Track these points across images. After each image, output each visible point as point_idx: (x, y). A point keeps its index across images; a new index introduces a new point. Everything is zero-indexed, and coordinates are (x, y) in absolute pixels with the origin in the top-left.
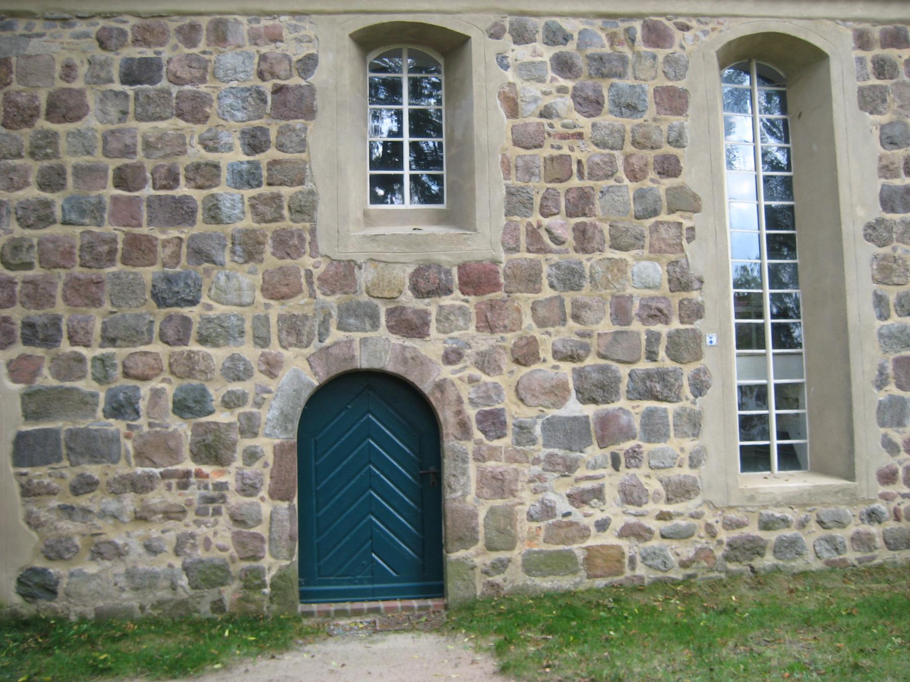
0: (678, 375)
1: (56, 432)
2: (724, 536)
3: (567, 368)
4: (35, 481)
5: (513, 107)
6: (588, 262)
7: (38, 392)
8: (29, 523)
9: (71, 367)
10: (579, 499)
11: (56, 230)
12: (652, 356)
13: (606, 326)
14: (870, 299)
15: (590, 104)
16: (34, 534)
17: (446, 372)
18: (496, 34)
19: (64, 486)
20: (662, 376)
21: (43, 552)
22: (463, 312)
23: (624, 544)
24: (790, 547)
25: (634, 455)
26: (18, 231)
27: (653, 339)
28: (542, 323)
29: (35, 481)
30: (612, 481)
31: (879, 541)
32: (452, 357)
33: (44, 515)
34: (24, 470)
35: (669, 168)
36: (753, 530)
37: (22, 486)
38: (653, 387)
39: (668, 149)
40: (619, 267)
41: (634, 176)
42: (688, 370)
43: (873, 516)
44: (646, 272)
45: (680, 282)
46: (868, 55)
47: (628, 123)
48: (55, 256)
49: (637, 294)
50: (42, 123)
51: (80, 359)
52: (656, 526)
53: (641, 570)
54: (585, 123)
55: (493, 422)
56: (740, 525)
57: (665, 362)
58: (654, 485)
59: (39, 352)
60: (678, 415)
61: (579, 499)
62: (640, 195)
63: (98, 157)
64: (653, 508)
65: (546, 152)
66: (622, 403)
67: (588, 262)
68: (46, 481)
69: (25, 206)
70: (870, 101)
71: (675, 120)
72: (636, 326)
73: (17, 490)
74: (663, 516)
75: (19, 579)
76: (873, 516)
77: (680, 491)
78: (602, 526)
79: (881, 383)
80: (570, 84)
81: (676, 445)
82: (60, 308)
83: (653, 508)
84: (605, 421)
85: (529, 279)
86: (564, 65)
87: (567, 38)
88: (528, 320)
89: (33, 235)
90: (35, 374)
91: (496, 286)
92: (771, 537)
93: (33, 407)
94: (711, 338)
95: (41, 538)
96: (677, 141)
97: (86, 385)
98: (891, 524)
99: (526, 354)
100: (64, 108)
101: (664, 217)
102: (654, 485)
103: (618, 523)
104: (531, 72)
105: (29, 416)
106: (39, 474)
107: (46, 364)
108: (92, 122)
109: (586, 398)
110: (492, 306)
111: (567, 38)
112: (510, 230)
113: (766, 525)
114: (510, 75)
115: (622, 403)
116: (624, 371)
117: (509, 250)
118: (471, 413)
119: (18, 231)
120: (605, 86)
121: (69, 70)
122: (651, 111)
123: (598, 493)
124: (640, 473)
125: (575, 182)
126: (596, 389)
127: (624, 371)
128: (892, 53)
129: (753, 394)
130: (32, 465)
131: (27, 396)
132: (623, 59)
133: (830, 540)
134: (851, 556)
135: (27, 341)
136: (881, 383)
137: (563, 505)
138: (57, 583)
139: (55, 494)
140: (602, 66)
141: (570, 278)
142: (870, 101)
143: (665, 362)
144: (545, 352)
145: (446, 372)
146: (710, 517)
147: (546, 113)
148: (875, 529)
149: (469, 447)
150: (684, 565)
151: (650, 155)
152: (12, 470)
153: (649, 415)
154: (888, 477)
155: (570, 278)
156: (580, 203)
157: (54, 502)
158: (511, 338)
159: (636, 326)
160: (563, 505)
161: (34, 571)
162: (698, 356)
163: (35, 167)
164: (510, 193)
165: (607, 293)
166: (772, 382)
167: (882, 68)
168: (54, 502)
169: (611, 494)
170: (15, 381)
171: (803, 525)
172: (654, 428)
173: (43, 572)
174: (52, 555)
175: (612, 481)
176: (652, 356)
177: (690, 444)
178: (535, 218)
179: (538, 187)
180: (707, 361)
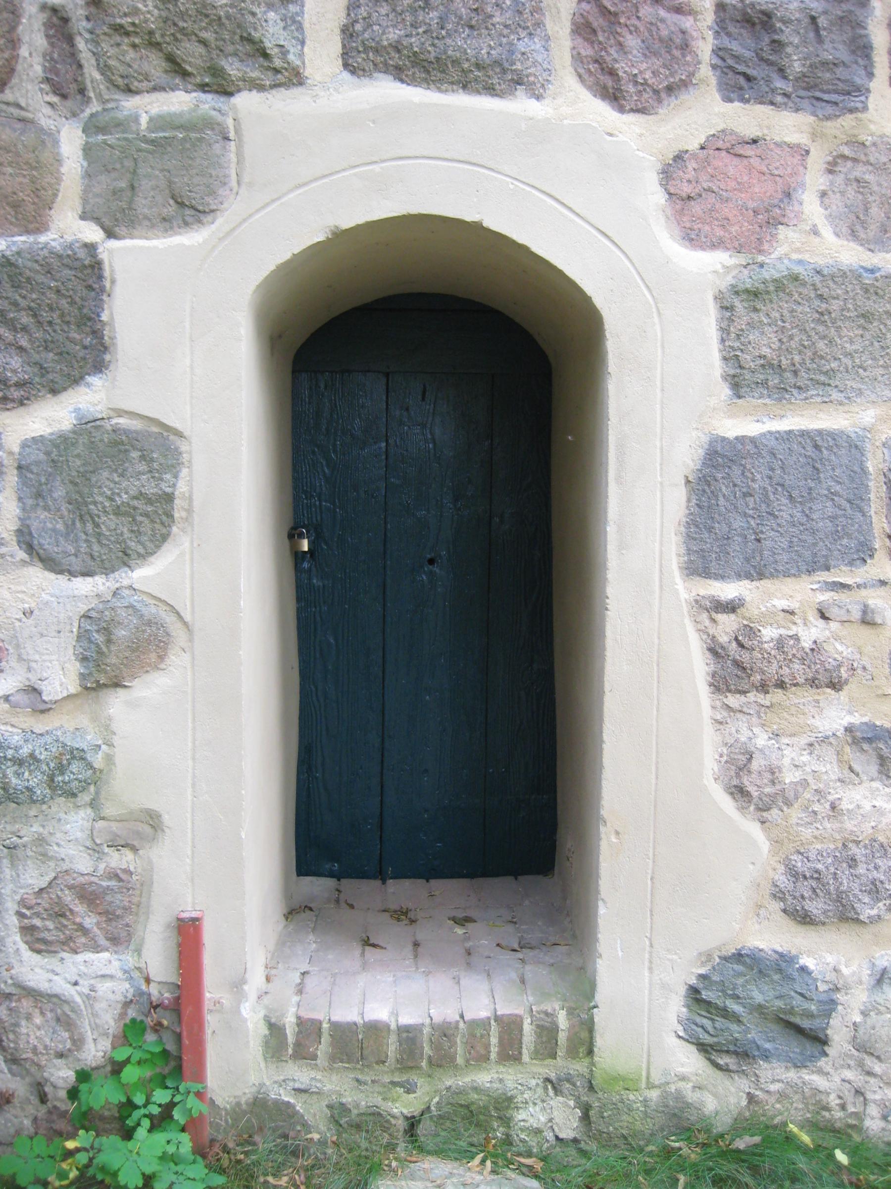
1: (854, 445)
4: (769, 633)
7: (786, 285)
8: (739, 792)
16: (754, 829)
21: (778, 895)
29: (769, 633)
33: (793, 761)
34: (728, 590)
37: (715, 651)
59: (788, 126)
68: (811, 632)
73: (700, 666)
75: (694, 994)
90: (772, 217)
93: (764, 343)
95: (777, 842)
105: (744, 379)
106: (784, 605)
107: (814, 178)
130: (757, 572)
131: (745, 301)
135: (739, 82)
138: (830, 1006)
139: (836, 685)
152: (686, 590)
157: (835, 715)
161: (745, 960)
168: (835, 715)
170: (692, 238)
173: (782, 967)
174: (815, 907)
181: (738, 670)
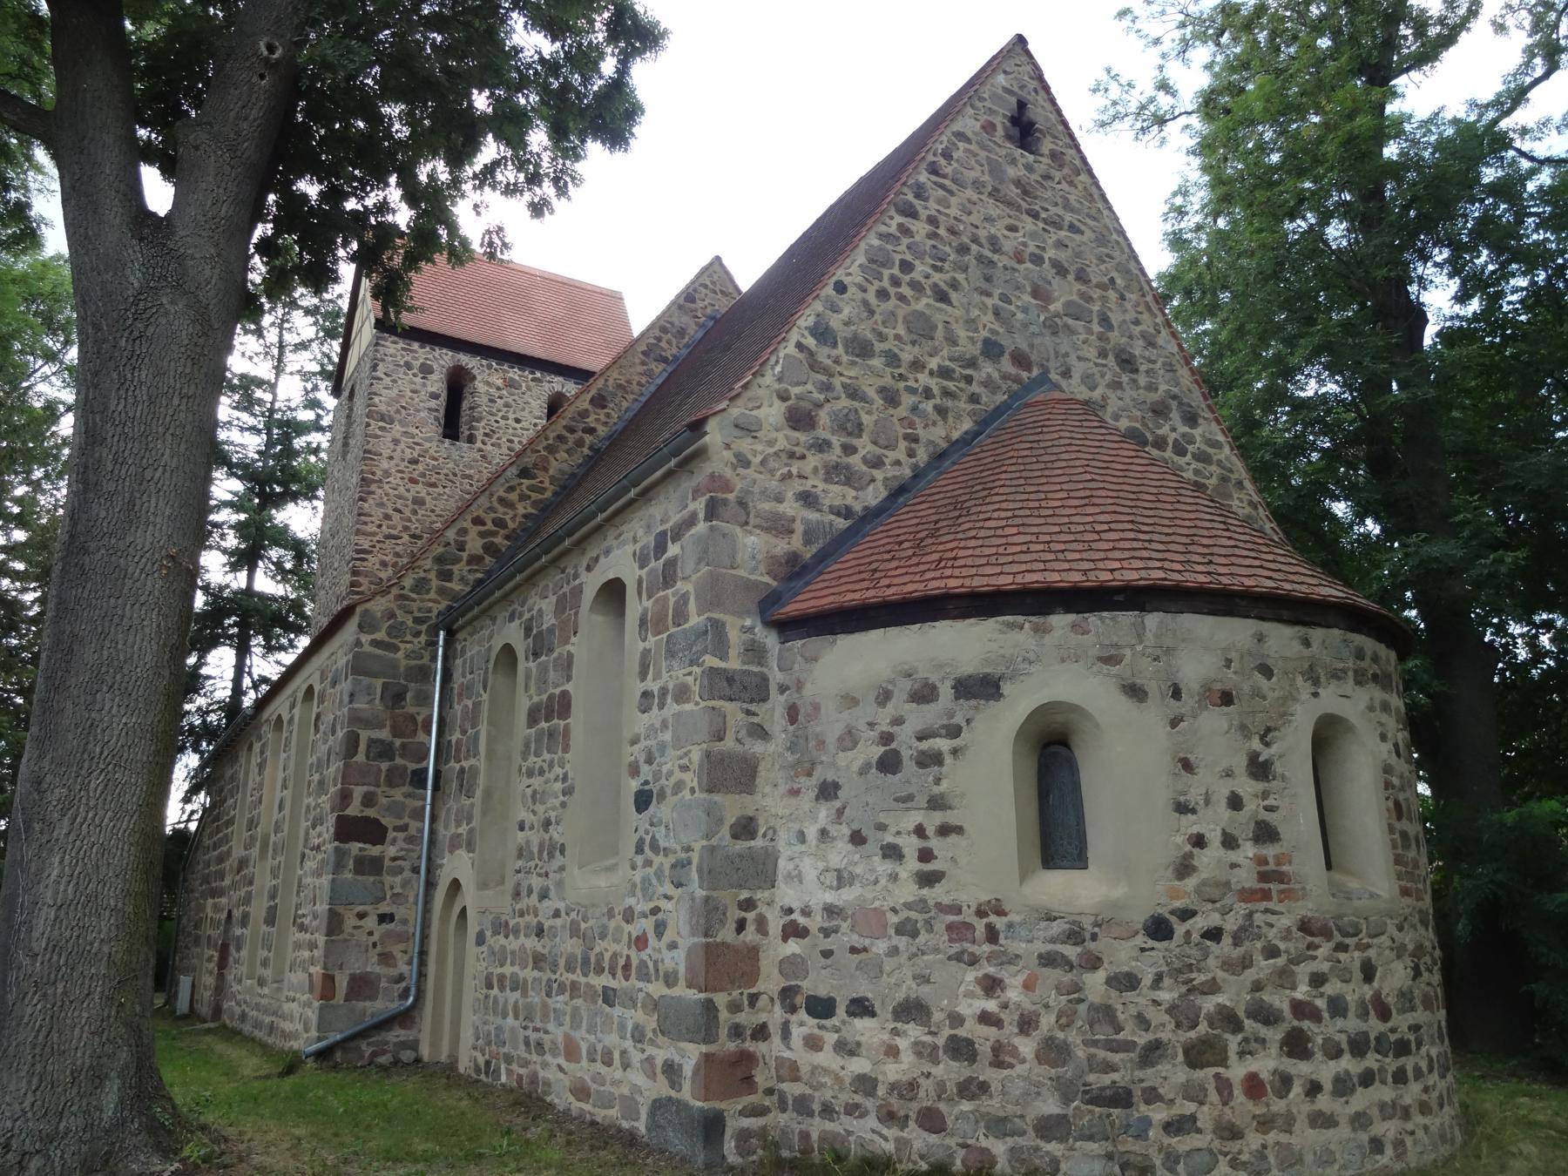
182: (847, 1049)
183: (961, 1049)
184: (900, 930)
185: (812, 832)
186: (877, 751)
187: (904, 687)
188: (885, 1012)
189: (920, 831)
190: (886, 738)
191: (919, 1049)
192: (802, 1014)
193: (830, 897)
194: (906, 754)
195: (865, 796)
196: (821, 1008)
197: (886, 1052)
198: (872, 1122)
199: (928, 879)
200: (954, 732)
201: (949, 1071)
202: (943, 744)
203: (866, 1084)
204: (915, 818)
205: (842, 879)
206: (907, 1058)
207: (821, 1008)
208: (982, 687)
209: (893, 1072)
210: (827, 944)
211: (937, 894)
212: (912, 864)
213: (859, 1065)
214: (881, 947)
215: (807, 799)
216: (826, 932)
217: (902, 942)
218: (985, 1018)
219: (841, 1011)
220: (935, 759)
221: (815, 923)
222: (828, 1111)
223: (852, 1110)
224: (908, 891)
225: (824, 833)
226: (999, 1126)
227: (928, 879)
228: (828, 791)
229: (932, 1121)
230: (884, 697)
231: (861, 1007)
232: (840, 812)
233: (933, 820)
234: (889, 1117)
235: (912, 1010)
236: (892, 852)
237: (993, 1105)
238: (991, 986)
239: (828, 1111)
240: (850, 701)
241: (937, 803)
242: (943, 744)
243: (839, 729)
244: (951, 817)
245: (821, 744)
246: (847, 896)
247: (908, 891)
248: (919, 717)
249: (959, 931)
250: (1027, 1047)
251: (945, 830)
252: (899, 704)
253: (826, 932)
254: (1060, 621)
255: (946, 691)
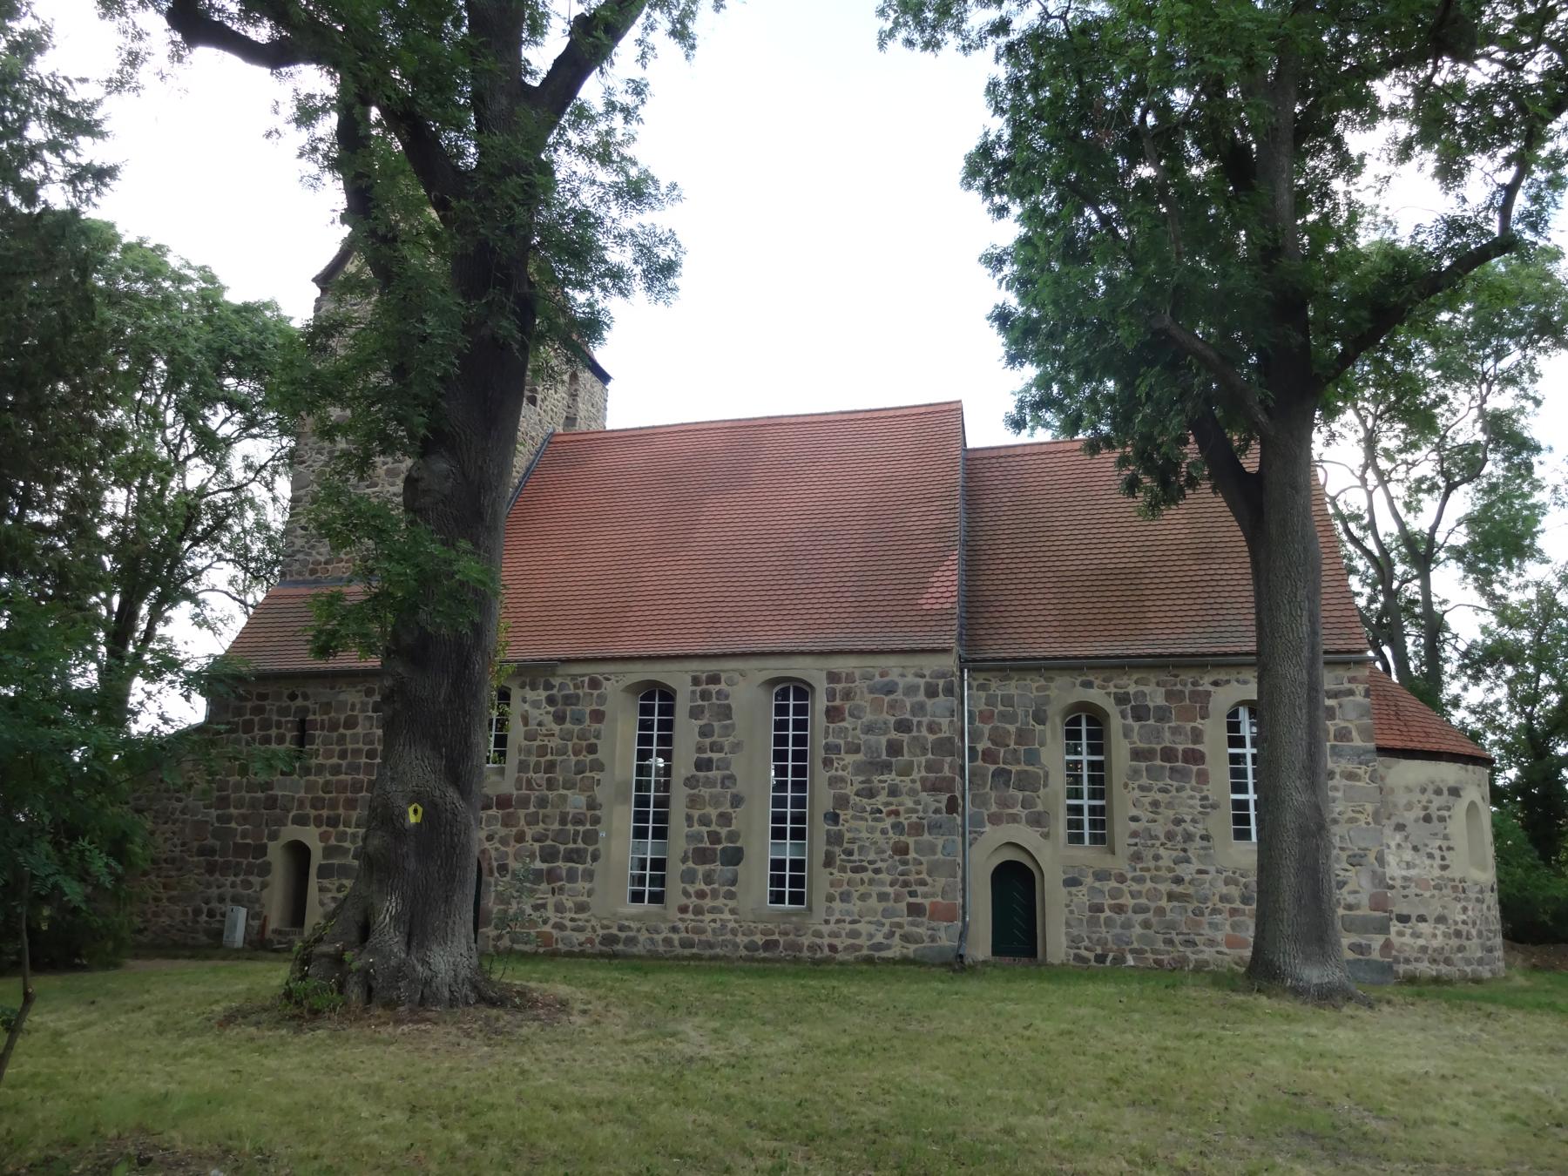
0: (586, 850)
2: (601, 932)
3: (537, 846)
5: (526, 720)
6: (551, 795)
9: (342, 837)
10: (536, 908)
11: (343, 777)
12: (575, 842)
13: (556, 826)
14: (684, 816)
15: (560, 718)
17: (487, 845)
18: (522, 687)
19: (334, 887)
20: (578, 851)
22: (495, 817)
23: (554, 932)
24: (632, 941)
25: (561, 889)
26: (329, 777)
27: (577, 833)
28: (528, 824)
30: (551, 901)
31: (676, 943)
32: (490, 838)
35: (592, 749)
36: (614, 931)
38: (574, 856)
39: (593, 741)
40: (564, 798)
41: (575, 754)
42: (591, 849)
43: (674, 929)
44: (576, 801)
45: (592, 805)
46: (698, 689)
47: (577, 728)
48: (342, 787)
49: (571, 811)
50: (342, 730)
51: (345, 833)
52: (568, 924)
53: (560, 946)
54: (556, 728)
55: (503, 868)
56: (608, 927)
57: (580, 845)
58: (569, 904)
60: (584, 871)
61: (536, 908)
62: (577, 763)
63: (360, 745)
64: (569, 915)
65: (538, 743)
66: (560, 864)
67: (551, 795)
69: (332, 766)
70: (695, 713)
71: (597, 726)
72: (570, 827)
74: (572, 920)
76: (674, 929)
77: (581, 908)
78: (545, 922)
79: (684, 860)
80: (552, 709)
81: (581, 885)
82: (341, 811)
83: (569, 915)
84: (550, 871)
85: (524, 802)
86: (551, 700)
87: (553, 687)
88: (522, 822)
89: (335, 778)
91: (510, 806)
92: (623, 935)
94: (603, 834)
96: (597, 737)
97: (347, 844)
98: (684, 935)
99: (520, 838)
100: (351, 723)
101: (588, 774)
102: (569, 904)
103: (551, 922)
104: (536, 704)
106: (326, 883)
108: (359, 730)
109: (543, 861)
110: (509, 815)
111: (553, 687)
112: (519, 780)
113: (621, 929)
114: (527, 707)
115: (560, 864)
116: (562, 847)
117: (519, 789)
118: (495, 864)
119: (329, 777)
120: (568, 709)
121: (353, 705)
122: (588, 722)
123: (544, 906)
124: (564, 898)
125: (549, 757)
126: (549, 855)
127: (562, 847)
128: (711, 687)
129: (778, 865)
131: (325, 849)
132: (578, 696)
133: (652, 940)
134: (661, 949)
136: (684, 860)
137: (529, 910)
140: (569, 700)
141: (543, 803)
142: (695, 713)
143: (580, 845)
144: (528, 837)
145: (487, 845)
146: (594, 922)
147: (540, 724)
148: (675, 937)
149: (492, 880)
150: (581, 944)
151: (584, 743)
153: (570, 869)
154: (684, 909)
155: (543, 803)
156: (551, 766)
158: (514, 830)
159: (570, 827)
160: (529, 910)
162: (596, 842)
163: (337, 748)
164: (521, 762)
165: (557, 812)
166: (649, 857)
167: (705, 695)
169: (550, 907)
171: (639, 930)
172: (572, 876)
175: (551, 901)
176: (575, 842)
177: (588, 886)
178: (531, 774)
179: (533, 759)
180: (600, 845)
181: (321, 890)
182: (1416, 935)
183: (1458, 934)
184: (1435, 887)
185: (1393, 845)
186: (1422, 813)
187: (1431, 788)
188: (1431, 920)
189: (1440, 848)
190: (1426, 808)
191: (1445, 935)
192: (1395, 922)
193: (1404, 873)
194: (1434, 817)
195: (1418, 832)
196: (1404, 919)
197: (1433, 936)
198: (1426, 964)
199: (1444, 868)
200: (1449, 809)
201: (1454, 942)
202: (1446, 813)
203: (1424, 949)
204: (1438, 843)
205: (1409, 865)
206: (1440, 938)
207: (1404, 919)
208: (1455, 792)
209: (1436, 943)
210: (1405, 892)
211: (1446, 873)
212: (1439, 861)
213: (1421, 942)
214: (1427, 894)
215: (1388, 831)
216: (1404, 888)
217: (1436, 892)
218: (1464, 922)
219: (1414, 919)
220: (1442, 819)
221: (1398, 883)
222: (1407, 961)
223: (1417, 960)
224: (1437, 872)
225: (1399, 846)
226: (1468, 962)
227: (1444, 868)
228: (1400, 827)
229: (1448, 961)
230: (1423, 791)
231: (1422, 919)
232: (1407, 838)
233: (1445, 844)
234: (1434, 961)
235: (1441, 919)
236: (1430, 856)
237: (1467, 954)
238: (1465, 909)
239: (1407, 961)
240: (1409, 789)
241: (1446, 837)
242: (1446, 813)
243: (1404, 801)
244: (1451, 843)
245: (1395, 806)
246: (1412, 873)
247: (1437, 872)
248: (1438, 801)
249: (1455, 888)
250: (1474, 932)
251: (1449, 848)
252: (1430, 794)
253: (1404, 888)
254: (1470, 767)
255: (1446, 792)
